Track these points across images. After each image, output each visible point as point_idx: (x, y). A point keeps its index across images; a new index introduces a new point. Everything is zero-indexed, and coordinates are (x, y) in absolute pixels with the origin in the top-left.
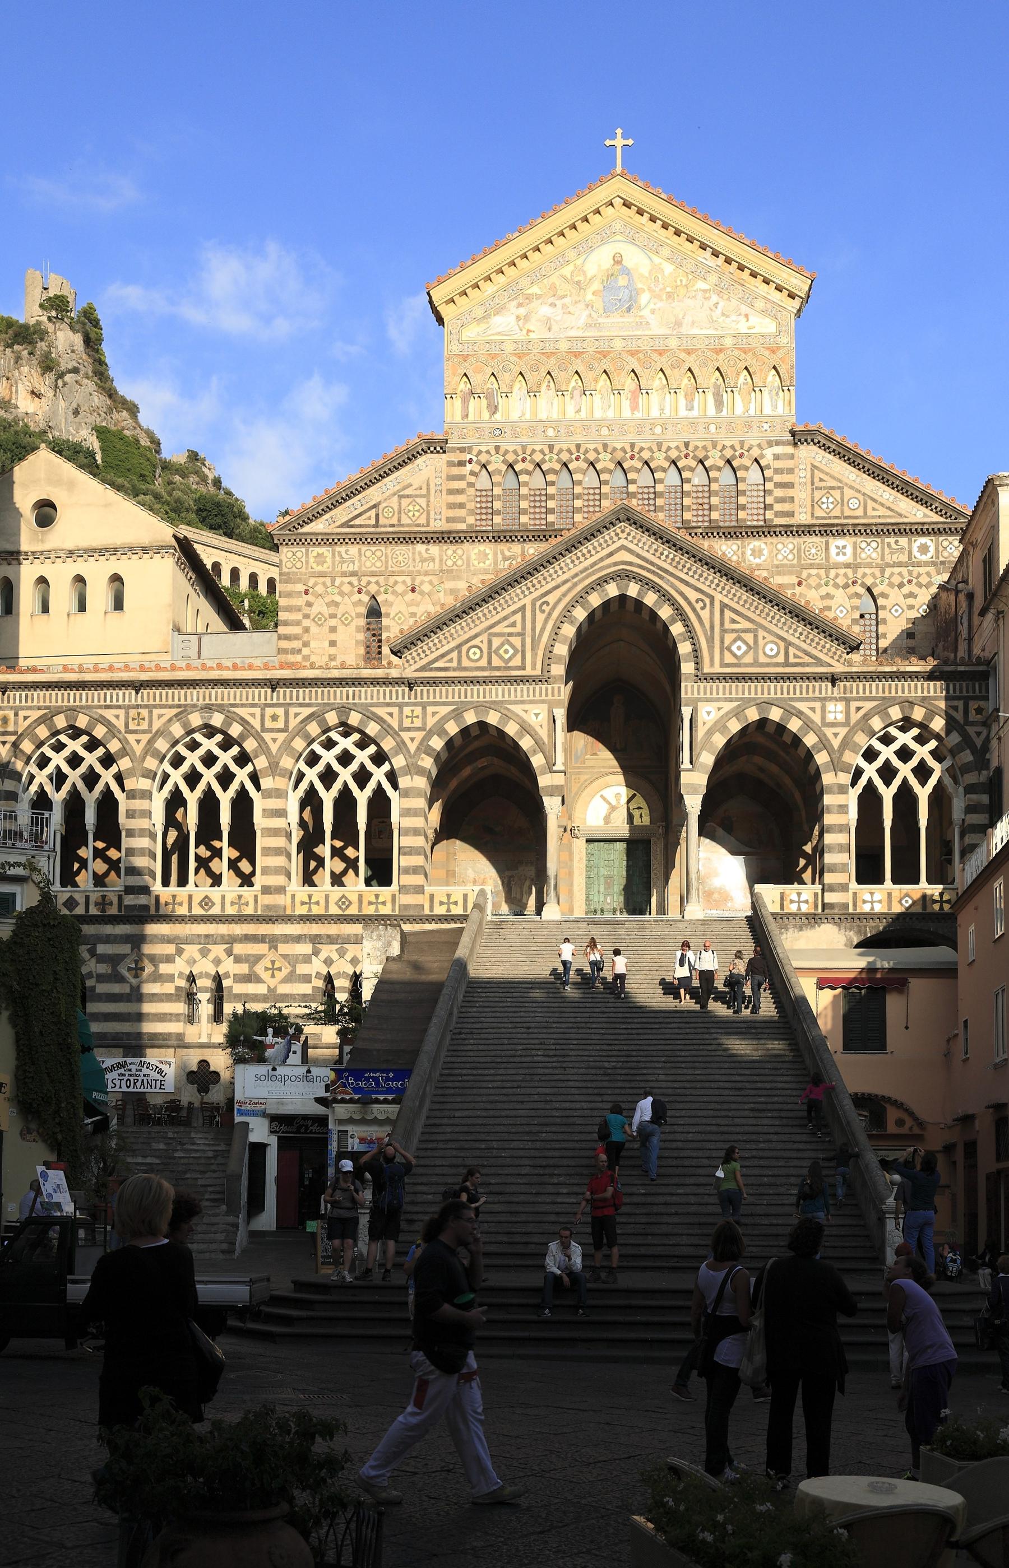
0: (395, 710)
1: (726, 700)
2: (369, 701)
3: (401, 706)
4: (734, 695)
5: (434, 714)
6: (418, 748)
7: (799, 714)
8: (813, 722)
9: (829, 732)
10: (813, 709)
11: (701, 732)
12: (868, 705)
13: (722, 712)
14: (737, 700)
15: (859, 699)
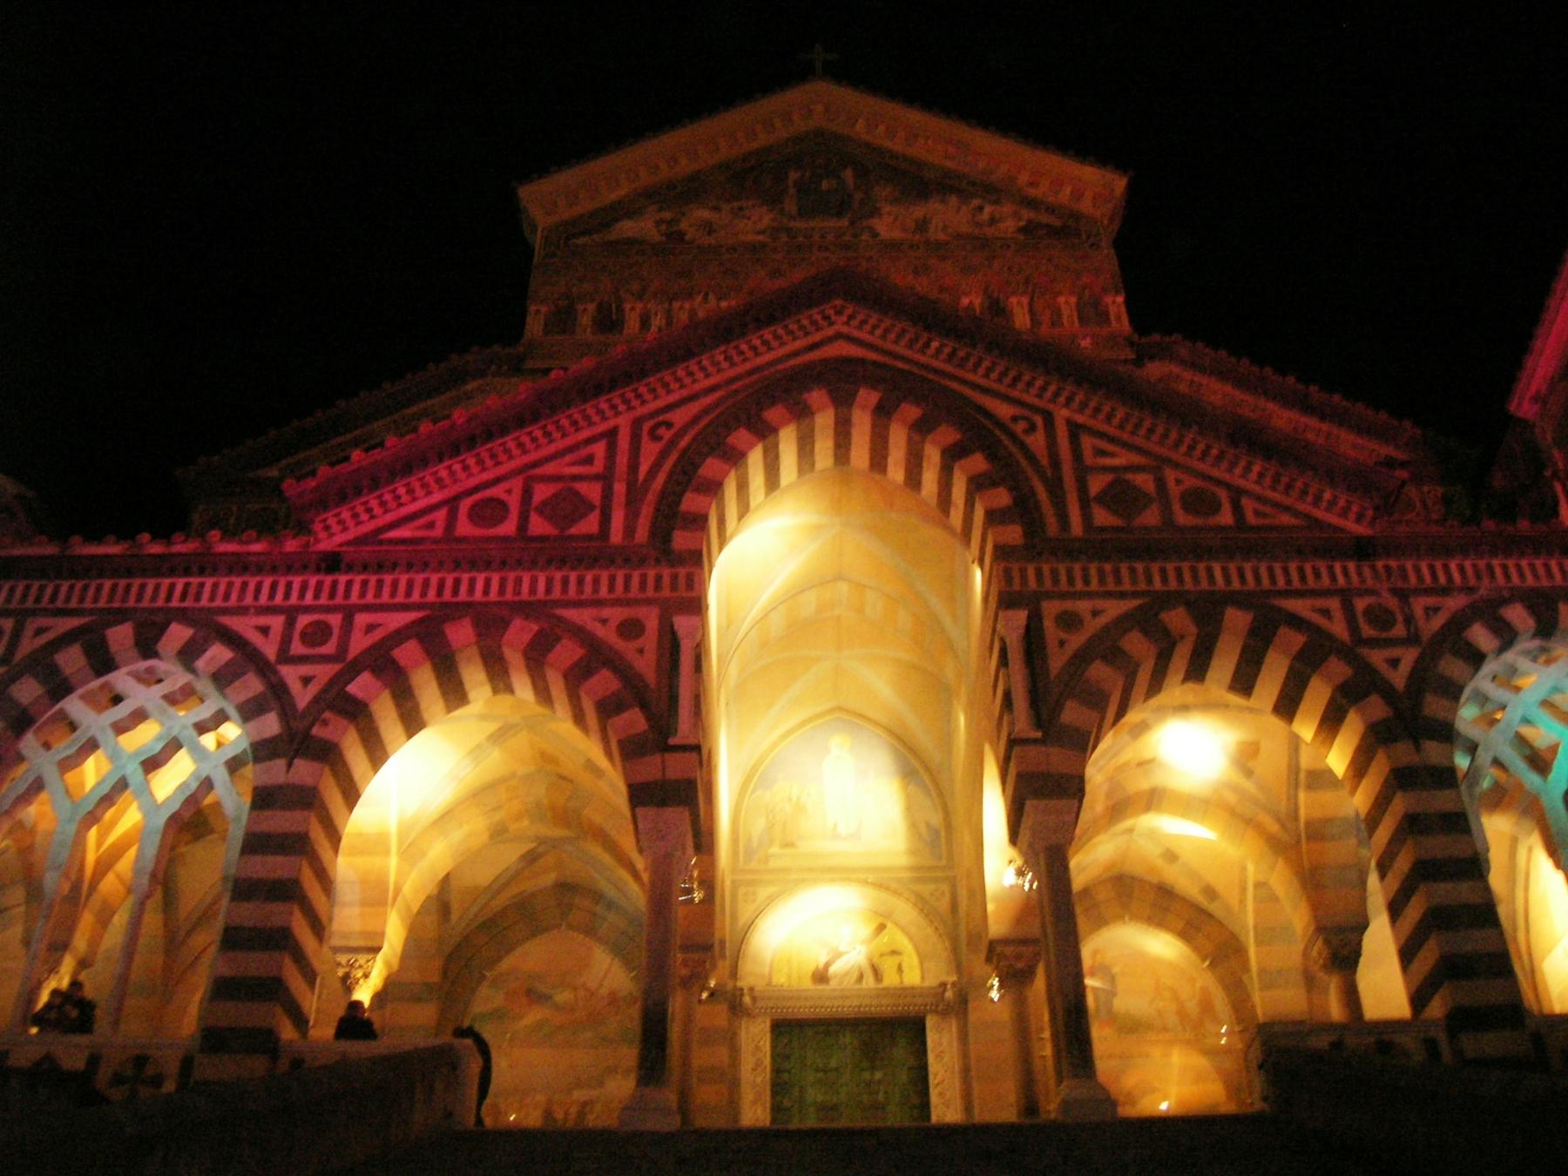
0: (277, 623)
1: (1109, 595)
2: (218, 602)
3: (291, 614)
4: (1127, 586)
5: (370, 628)
6: (316, 700)
7: (1296, 622)
8: (1330, 637)
9: (1377, 657)
10: (1326, 613)
11: (1056, 662)
12: (1455, 603)
13: (1103, 620)
14: (1135, 595)
15: (1427, 592)
